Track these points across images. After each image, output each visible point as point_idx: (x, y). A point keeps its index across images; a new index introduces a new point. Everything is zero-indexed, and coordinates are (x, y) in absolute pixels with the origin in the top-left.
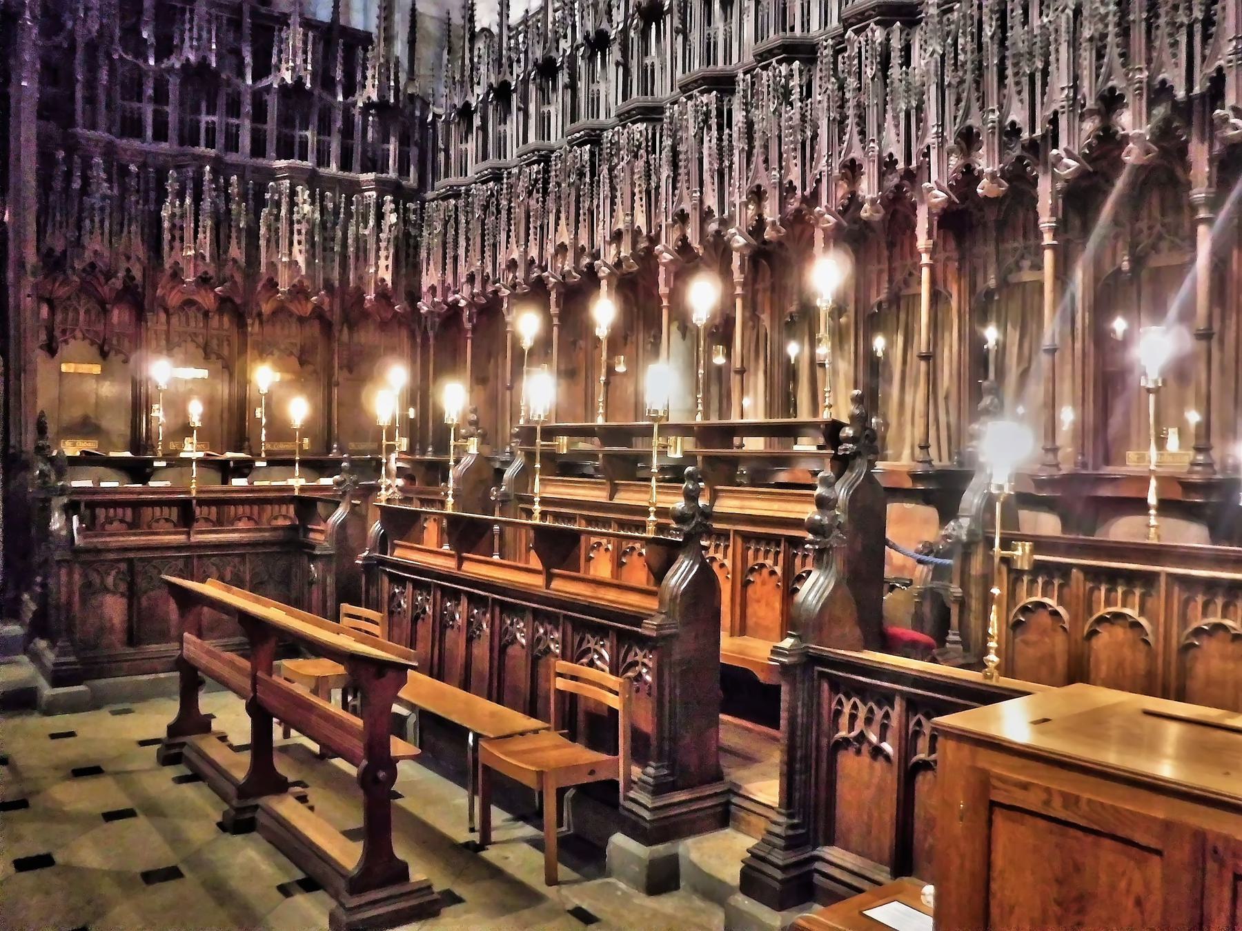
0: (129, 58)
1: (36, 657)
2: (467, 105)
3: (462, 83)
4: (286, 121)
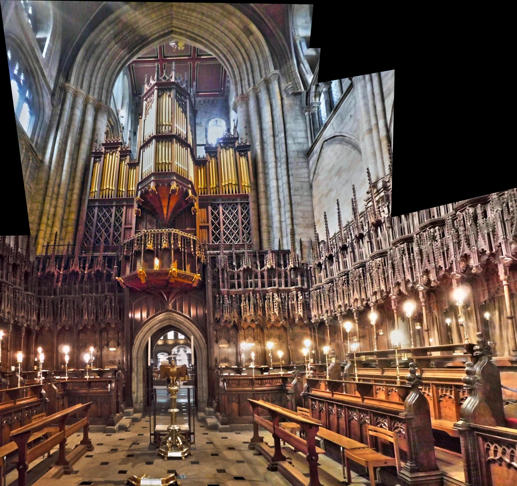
0: (231, 270)
1: (217, 417)
2: (320, 263)
3: (317, 257)
4: (269, 277)
